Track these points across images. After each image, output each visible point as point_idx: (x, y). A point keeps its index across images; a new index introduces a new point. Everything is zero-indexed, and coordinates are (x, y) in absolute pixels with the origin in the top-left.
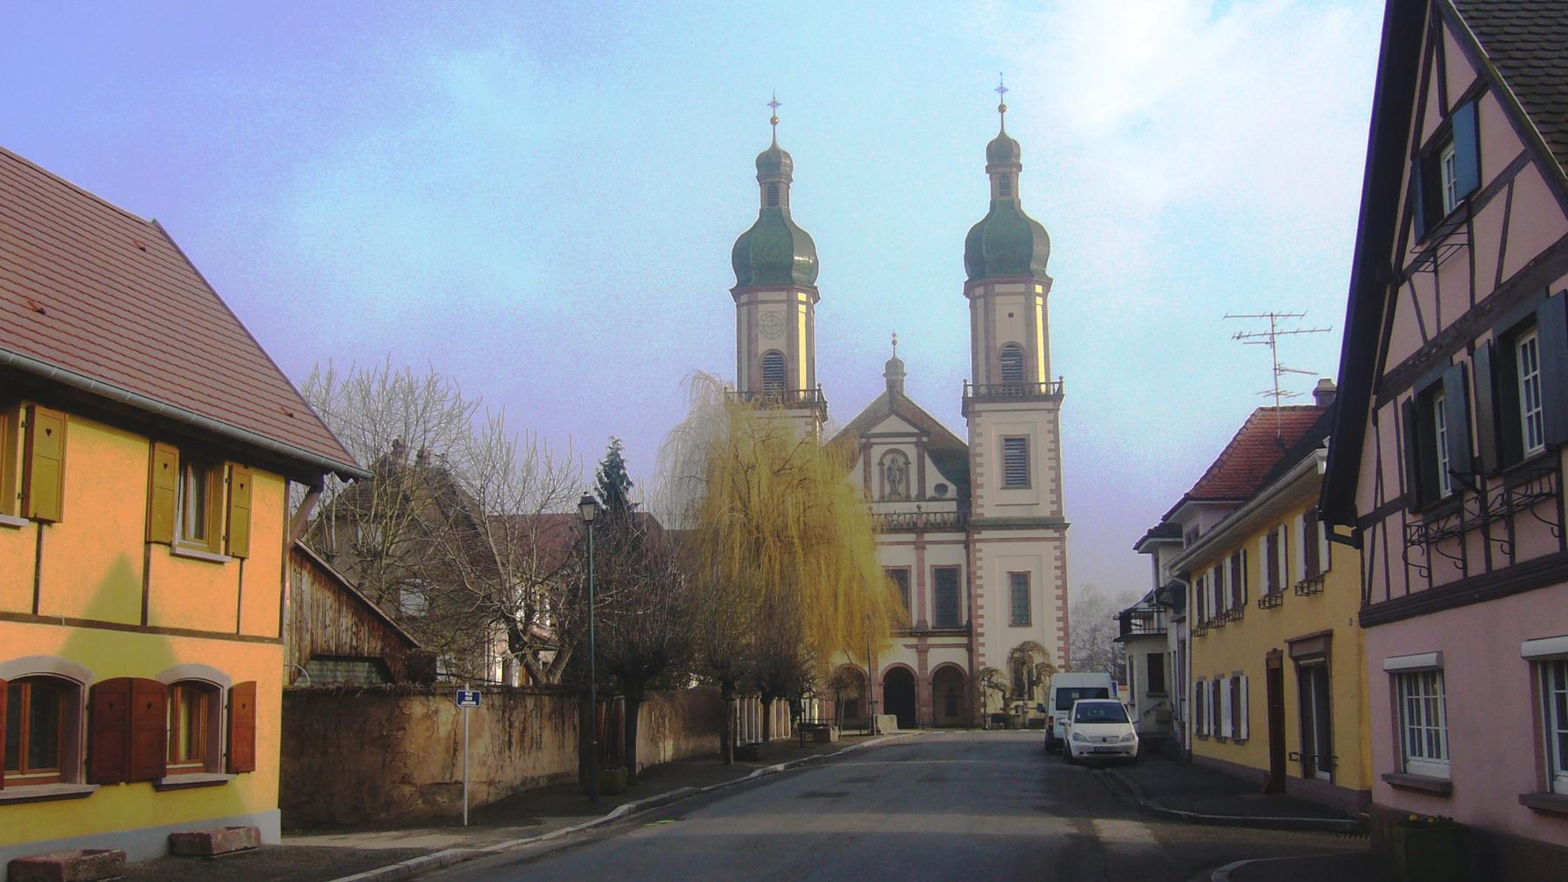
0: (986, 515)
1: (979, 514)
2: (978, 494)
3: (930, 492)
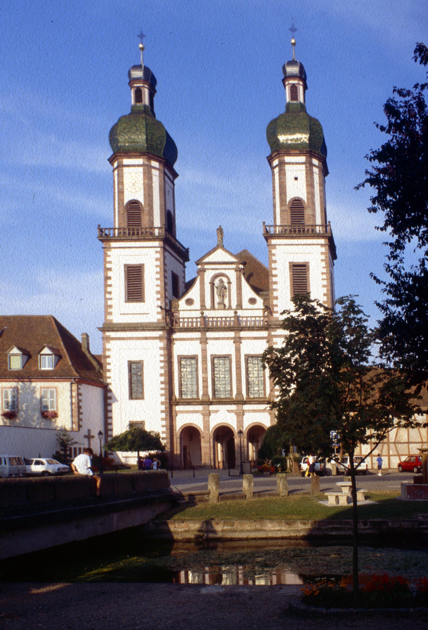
3: (246, 304)
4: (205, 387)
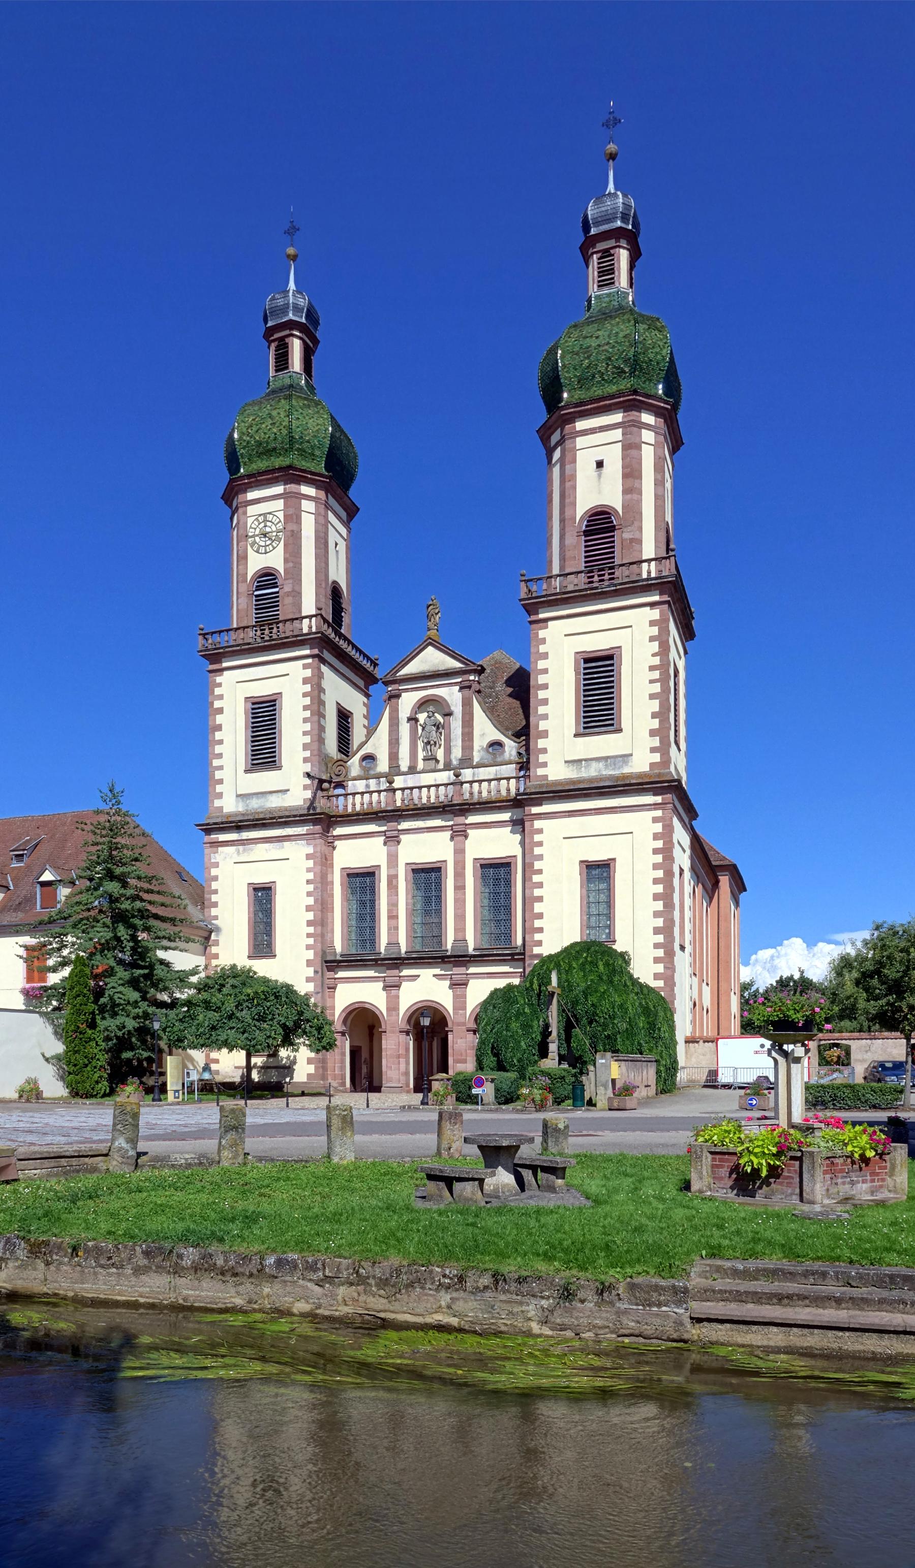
0: (551, 778)
4: (393, 929)
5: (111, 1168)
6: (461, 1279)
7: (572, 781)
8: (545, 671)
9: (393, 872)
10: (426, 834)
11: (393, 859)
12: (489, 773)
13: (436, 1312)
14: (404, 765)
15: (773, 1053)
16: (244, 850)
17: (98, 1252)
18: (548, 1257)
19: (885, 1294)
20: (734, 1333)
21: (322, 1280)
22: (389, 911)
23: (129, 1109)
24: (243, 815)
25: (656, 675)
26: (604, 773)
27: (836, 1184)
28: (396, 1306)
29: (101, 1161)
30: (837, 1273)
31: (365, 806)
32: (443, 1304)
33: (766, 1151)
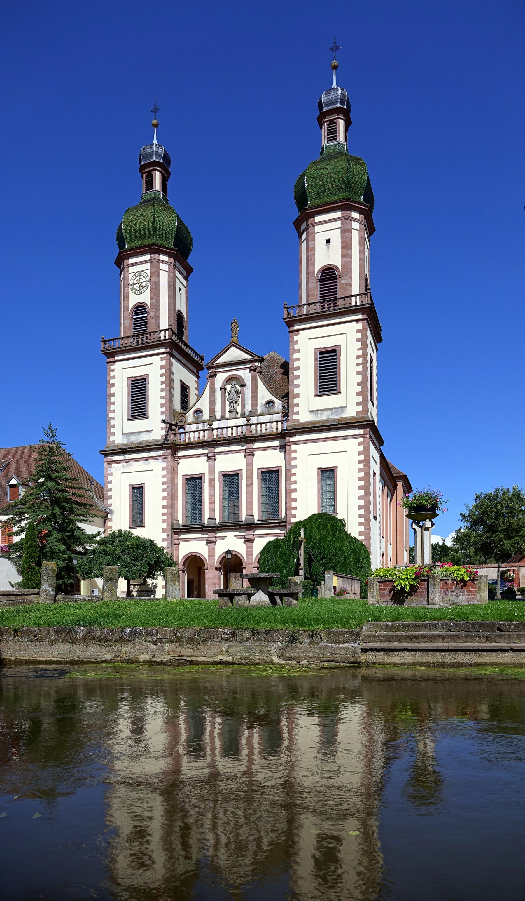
0: (301, 421)
1: (296, 420)
2: (295, 403)
4: (212, 510)
5: (40, 602)
6: (234, 634)
7: (313, 423)
8: (298, 360)
9: (212, 477)
10: (230, 454)
11: (212, 470)
12: (266, 419)
13: (220, 654)
14: (218, 416)
15: (414, 525)
16: (127, 466)
17: (29, 632)
18: (284, 623)
19: (468, 633)
20: (385, 657)
21: (156, 641)
22: (209, 499)
23: (50, 567)
24: (126, 445)
25: (360, 361)
26: (331, 417)
27: (448, 595)
28: (197, 653)
29: (35, 597)
30: (443, 624)
31: (196, 439)
32: (224, 649)
33: (409, 577)
